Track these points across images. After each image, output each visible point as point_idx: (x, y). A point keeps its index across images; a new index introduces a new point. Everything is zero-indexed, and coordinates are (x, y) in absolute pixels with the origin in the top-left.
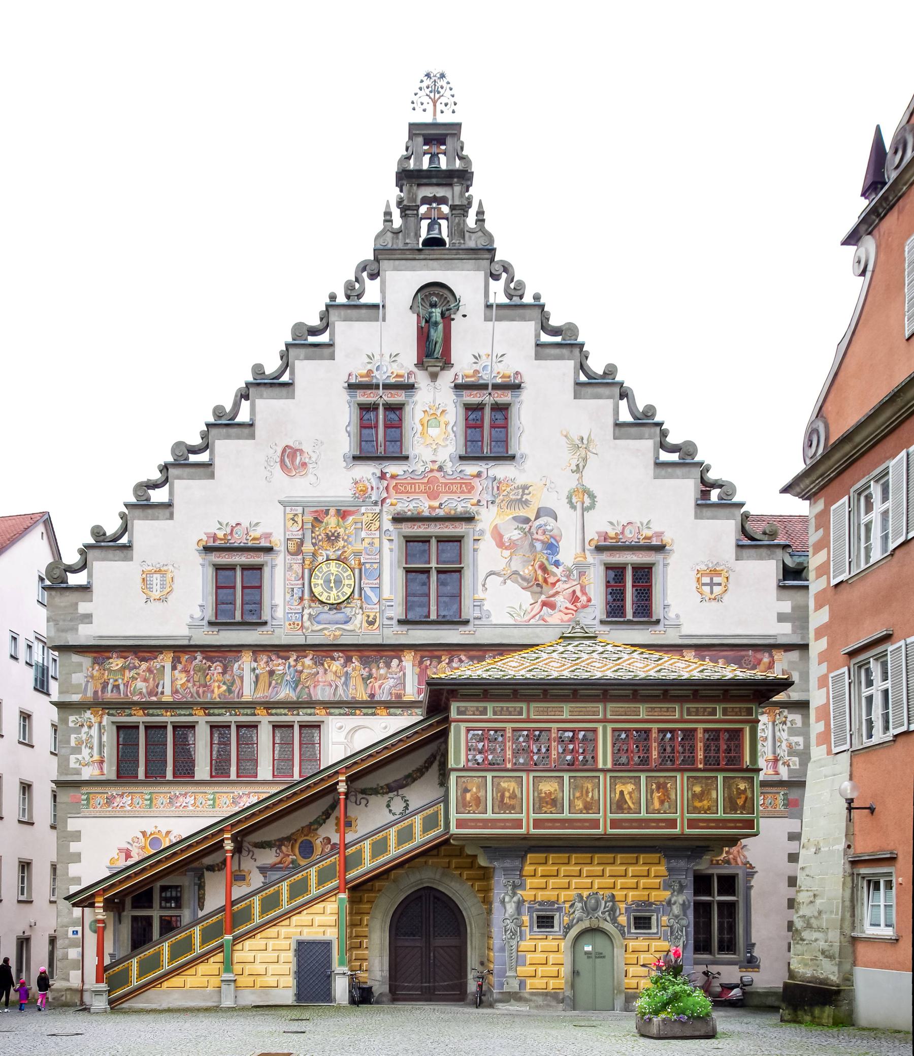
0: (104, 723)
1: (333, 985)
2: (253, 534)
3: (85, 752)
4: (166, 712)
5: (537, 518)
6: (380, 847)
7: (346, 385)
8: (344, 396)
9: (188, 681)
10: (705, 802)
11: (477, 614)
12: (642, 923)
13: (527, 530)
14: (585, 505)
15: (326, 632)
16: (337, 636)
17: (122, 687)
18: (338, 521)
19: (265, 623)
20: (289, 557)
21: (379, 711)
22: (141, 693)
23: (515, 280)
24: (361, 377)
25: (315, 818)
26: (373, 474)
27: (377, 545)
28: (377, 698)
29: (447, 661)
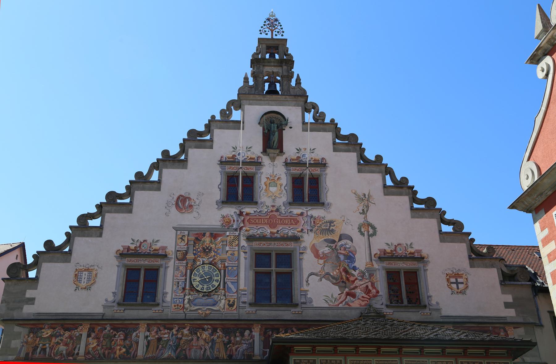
2: (154, 247)
5: (340, 240)
8: (218, 168)
9: (98, 345)
11: (303, 300)
13: (334, 247)
14: (369, 233)
15: (199, 311)
16: (207, 314)
17: (48, 350)
18: (211, 240)
20: (178, 262)
22: (61, 354)
23: (320, 111)
24: (229, 158)
26: (235, 212)
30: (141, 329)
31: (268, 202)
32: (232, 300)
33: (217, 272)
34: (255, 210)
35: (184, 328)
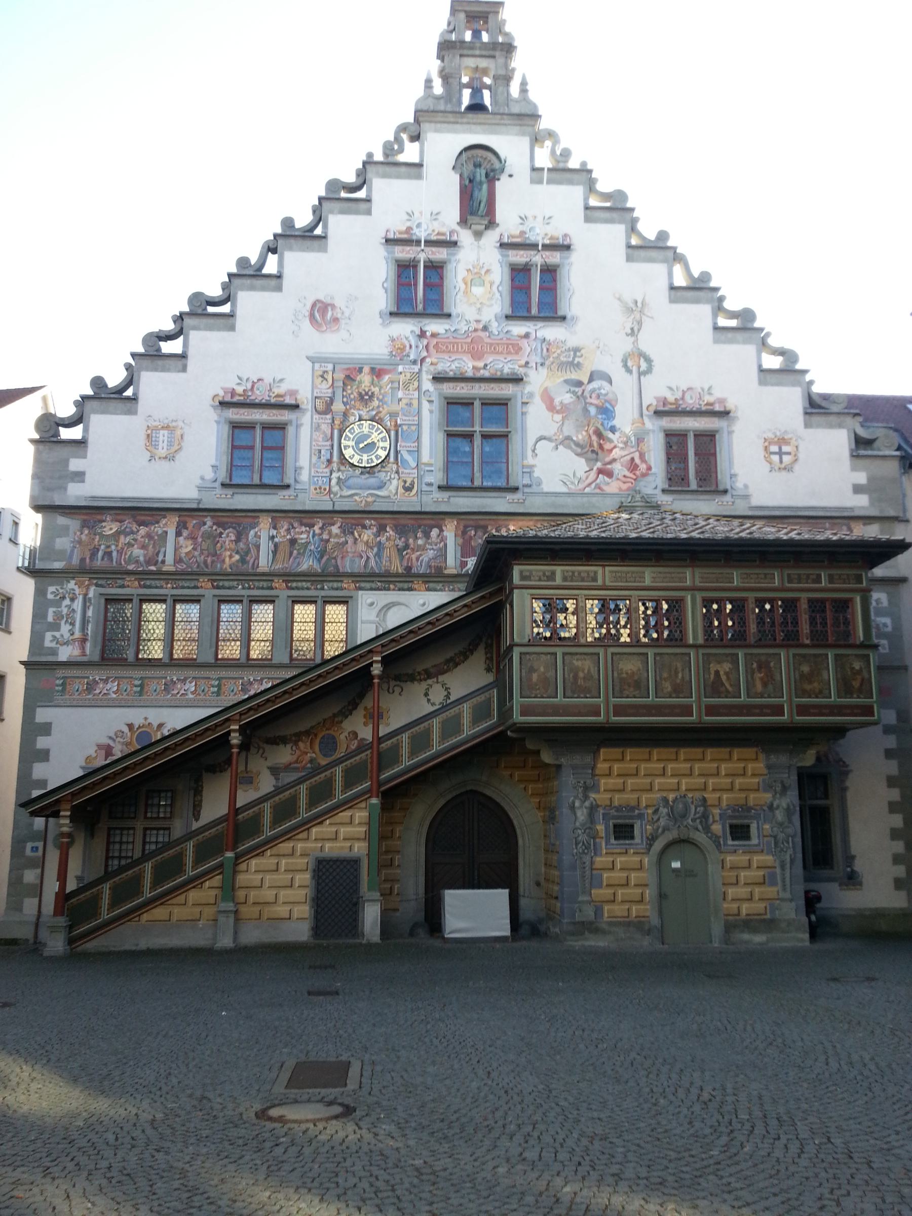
1: (361, 915)
2: (276, 391)
3: (65, 629)
4: (167, 584)
5: (590, 381)
6: (420, 742)
8: (381, 252)
9: (194, 549)
10: (816, 684)
11: (526, 481)
12: (740, 832)
13: (580, 393)
14: (641, 369)
15: (357, 498)
17: (115, 554)
20: (316, 416)
22: (137, 562)
24: (400, 233)
25: (338, 709)
26: (412, 332)
28: (414, 570)
30: (262, 525)
34: (447, 327)
35: (333, 525)
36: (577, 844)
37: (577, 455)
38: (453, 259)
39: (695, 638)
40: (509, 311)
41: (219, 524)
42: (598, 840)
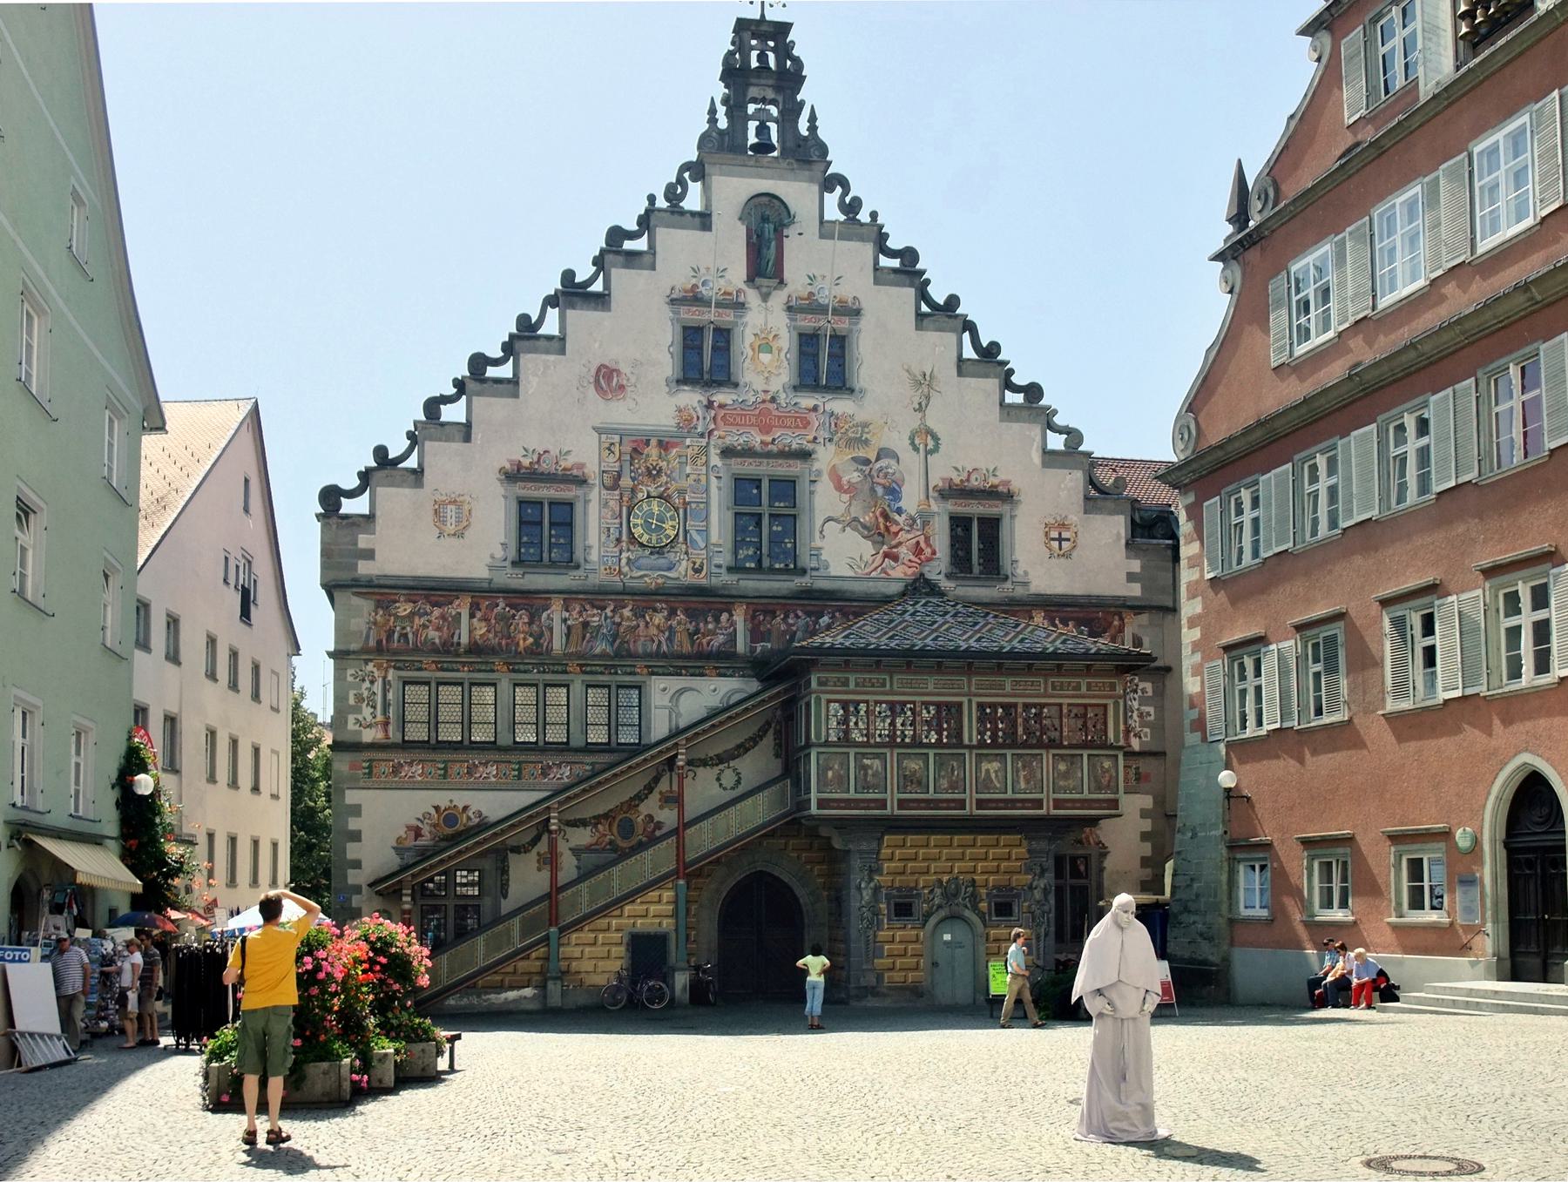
0: (390, 677)
2: (563, 464)
3: (367, 711)
4: (463, 667)
5: (878, 459)
7: (668, 300)
8: (667, 312)
9: (489, 631)
13: (867, 472)
15: (646, 579)
17: (410, 636)
19: (578, 567)
20: (605, 492)
21: (707, 672)
26: (699, 401)
27: (704, 482)
29: (782, 616)
31: (758, 383)
32: (698, 562)
33: (672, 513)
34: (735, 397)
35: (624, 607)
36: (862, 921)
37: (864, 537)
38: (740, 322)
39: (970, 739)
40: (796, 381)
41: (512, 606)
42: (881, 917)
